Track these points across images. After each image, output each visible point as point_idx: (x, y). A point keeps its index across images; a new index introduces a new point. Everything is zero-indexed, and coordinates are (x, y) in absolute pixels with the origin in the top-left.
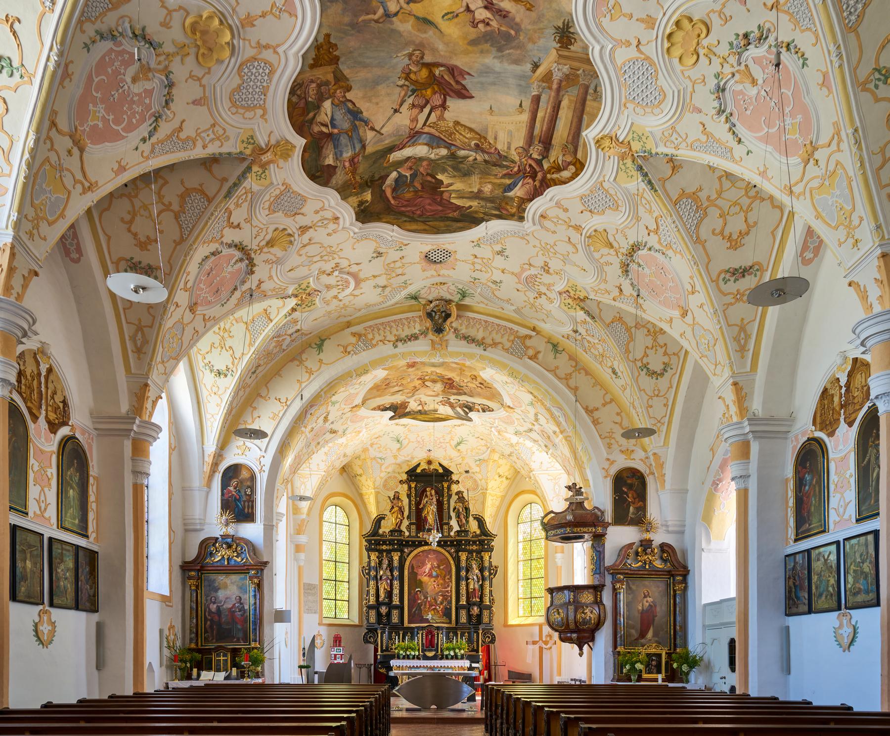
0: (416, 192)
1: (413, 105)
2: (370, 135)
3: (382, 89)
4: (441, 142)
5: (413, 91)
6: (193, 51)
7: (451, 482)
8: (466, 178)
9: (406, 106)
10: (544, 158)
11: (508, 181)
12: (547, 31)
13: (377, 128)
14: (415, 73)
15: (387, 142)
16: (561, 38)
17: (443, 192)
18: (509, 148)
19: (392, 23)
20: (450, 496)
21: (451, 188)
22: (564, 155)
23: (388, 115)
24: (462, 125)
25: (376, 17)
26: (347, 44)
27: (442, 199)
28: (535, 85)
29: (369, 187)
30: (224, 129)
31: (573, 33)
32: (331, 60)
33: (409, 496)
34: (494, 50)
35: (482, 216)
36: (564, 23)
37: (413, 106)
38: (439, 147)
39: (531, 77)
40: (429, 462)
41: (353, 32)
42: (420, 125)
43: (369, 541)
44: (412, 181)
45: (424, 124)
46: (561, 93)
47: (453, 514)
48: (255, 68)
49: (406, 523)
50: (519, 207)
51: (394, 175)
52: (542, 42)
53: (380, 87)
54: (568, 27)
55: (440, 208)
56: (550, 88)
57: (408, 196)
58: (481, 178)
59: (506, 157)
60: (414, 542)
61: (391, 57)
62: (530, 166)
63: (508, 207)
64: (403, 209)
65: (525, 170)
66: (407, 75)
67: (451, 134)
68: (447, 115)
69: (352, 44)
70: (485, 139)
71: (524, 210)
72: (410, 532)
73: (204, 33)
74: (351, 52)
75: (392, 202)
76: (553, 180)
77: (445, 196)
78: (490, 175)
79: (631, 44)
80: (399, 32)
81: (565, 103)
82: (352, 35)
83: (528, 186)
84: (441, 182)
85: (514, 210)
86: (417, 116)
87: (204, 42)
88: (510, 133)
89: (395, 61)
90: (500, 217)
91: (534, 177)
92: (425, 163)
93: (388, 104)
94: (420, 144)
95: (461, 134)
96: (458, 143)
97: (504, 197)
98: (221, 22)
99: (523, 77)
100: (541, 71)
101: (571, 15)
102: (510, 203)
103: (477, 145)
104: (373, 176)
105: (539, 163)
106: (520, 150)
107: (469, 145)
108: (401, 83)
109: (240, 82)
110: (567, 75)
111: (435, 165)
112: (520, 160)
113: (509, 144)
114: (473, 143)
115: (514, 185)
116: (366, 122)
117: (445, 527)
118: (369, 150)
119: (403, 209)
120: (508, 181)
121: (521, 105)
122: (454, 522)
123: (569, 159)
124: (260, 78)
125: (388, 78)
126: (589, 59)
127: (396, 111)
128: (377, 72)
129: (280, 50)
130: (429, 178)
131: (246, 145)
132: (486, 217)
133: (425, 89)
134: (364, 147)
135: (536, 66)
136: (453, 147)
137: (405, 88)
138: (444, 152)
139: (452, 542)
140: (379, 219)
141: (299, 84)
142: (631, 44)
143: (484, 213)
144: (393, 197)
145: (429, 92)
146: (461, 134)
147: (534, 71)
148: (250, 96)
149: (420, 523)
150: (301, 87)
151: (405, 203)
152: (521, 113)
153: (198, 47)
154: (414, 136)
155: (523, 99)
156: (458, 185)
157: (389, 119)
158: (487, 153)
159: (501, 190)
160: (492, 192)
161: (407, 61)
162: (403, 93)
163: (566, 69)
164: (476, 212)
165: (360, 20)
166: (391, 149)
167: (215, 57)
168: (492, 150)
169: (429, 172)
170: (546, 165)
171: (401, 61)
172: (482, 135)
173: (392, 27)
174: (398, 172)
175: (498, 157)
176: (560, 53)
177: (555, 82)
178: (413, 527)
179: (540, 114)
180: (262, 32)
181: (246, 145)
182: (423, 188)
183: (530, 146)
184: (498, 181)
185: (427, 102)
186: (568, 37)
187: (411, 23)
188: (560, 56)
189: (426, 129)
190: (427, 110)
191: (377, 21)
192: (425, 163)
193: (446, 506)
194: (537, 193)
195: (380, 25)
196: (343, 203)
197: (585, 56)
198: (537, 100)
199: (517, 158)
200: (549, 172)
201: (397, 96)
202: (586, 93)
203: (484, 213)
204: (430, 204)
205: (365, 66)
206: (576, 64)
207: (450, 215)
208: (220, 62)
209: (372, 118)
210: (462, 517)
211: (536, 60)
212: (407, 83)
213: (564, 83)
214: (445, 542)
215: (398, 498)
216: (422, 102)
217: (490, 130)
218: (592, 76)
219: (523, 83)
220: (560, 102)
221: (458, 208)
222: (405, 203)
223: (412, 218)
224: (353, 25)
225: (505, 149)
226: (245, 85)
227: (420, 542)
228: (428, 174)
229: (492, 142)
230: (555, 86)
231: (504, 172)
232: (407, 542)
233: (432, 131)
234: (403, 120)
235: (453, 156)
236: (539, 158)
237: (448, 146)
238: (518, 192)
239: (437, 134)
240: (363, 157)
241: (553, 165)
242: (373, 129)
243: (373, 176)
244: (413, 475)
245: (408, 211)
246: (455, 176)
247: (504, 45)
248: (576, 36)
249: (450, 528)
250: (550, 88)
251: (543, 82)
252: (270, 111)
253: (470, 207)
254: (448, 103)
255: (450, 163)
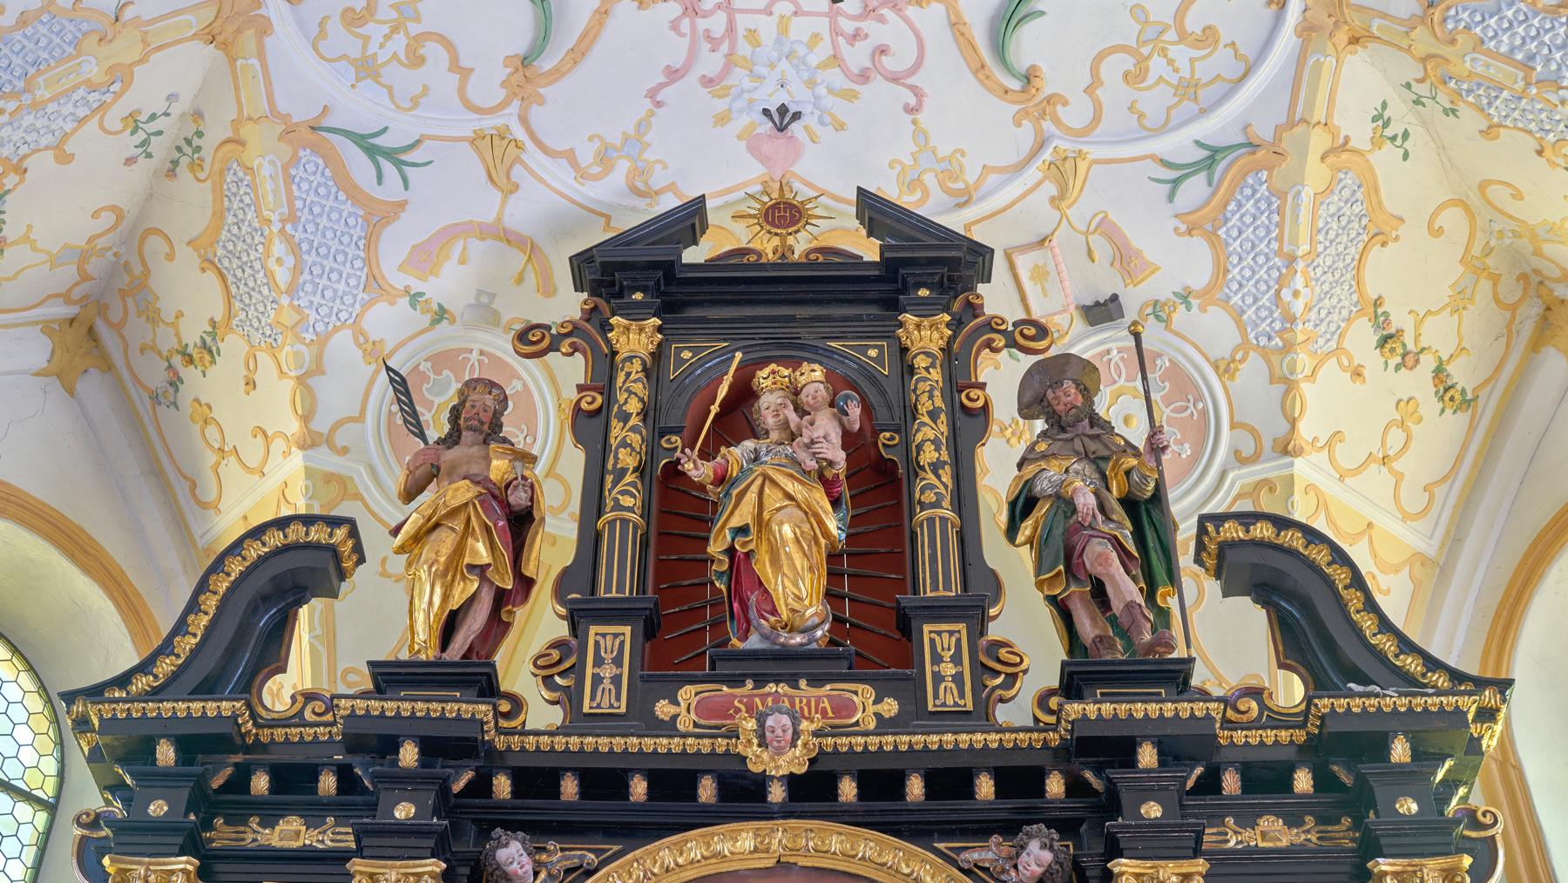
7: (973, 330)
20: (970, 421)
33: (590, 425)
40: (784, 214)
43: (126, 753)
47: (1013, 563)
49: (540, 622)
60: (604, 781)
72: (570, 699)
117: (941, 640)
122: (1027, 625)
139: (1019, 779)
149: (677, 599)
178: (613, 641)
193: (933, 487)
210: (1103, 559)
214: (950, 780)
215: (491, 431)
227: (673, 783)
232: (537, 779)
244: (640, 272)
249: (993, 666)
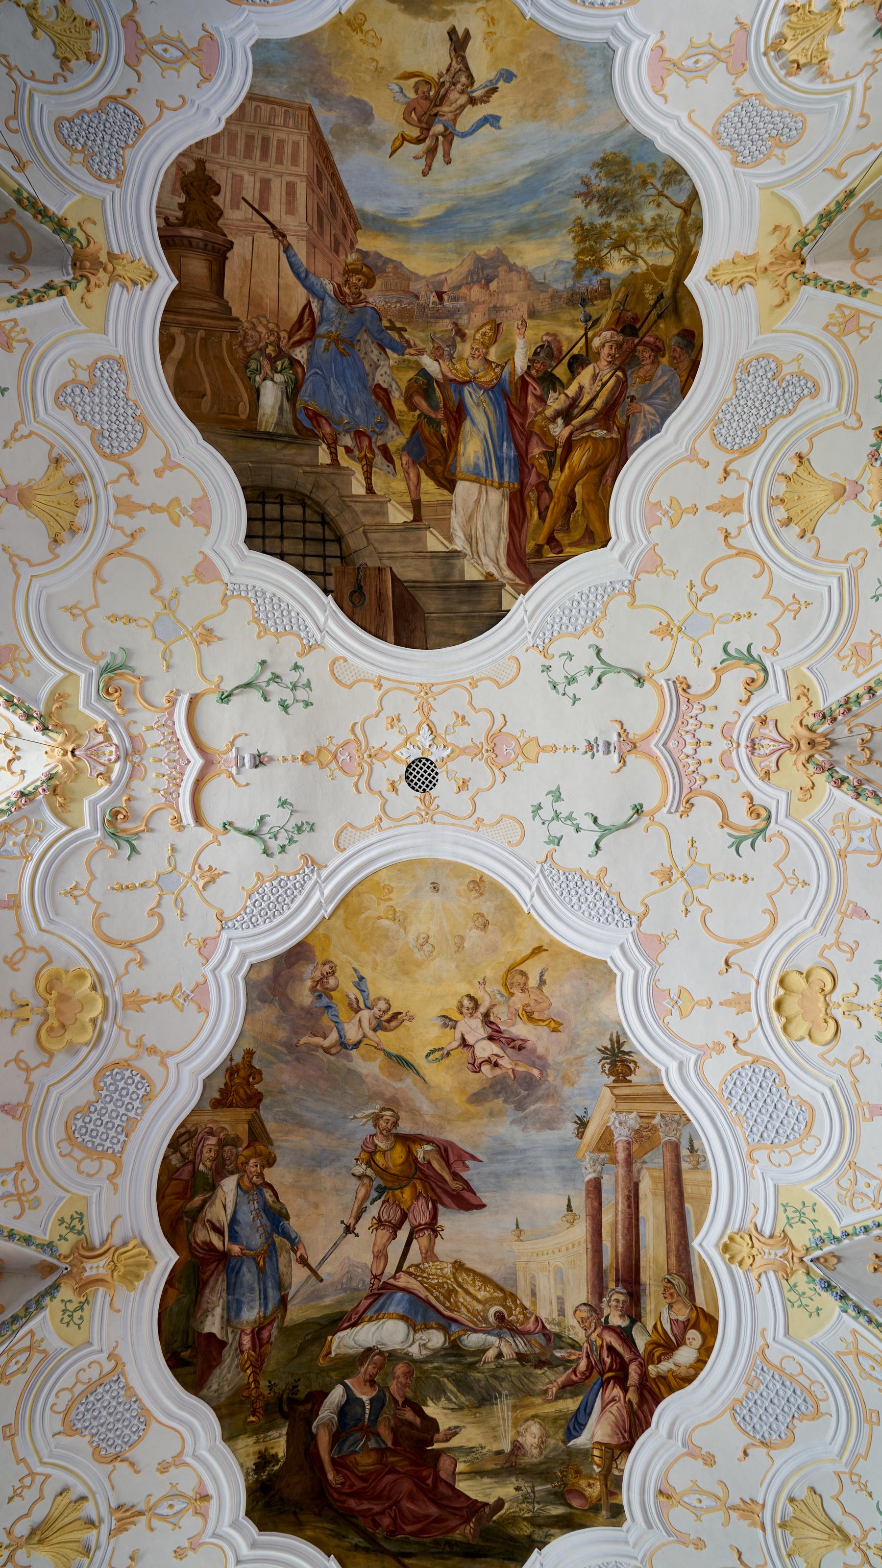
0: (382, 1451)
1: (379, 1220)
2: (298, 1275)
3: (327, 1177)
4: (432, 1313)
5: (381, 1190)
6: (36, 1019)
8: (484, 1411)
9: (366, 1221)
10: (633, 1322)
11: (571, 1405)
12: (588, 1059)
13: (314, 1266)
14: (384, 1153)
15: (329, 1302)
16: (613, 1064)
17: (439, 1453)
18: (562, 1312)
19: (349, 1059)
21: (455, 1442)
22: (670, 1306)
23: (336, 1241)
24: (469, 1271)
25: (326, 1043)
26: (278, 1076)
27: (437, 1479)
28: (587, 1162)
29: (285, 1416)
30: (36, 1181)
31: (628, 1053)
32: (249, 1098)
34: (510, 1107)
35: (526, 1529)
36: (611, 1040)
37: (380, 1223)
38: (427, 1327)
39: (577, 1148)
41: (288, 1058)
42: (391, 1269)
44: (374, 1420)
45: (399, 1269)
46: (636, 1166)
48: (123, 1083)
50: (606, 1474)
51: (337, 1394)
52: (584, 1080)
53: (323, 1172)
54: (620, 1045)
55: (433, 1510)
56: (614, 1161)
57: (366, 1462)
58: (515, 1408)
59: (559, 1336)
61: (345, 1117)
62: (610, 1348)
63: (583, 1483)
64: (352, 1503)
65: (602, 1362)
66: (370, 1155)
67: (451, 1292)
68: (441, 1247)
69: (285, 1077)
70: (514, 1297)
71: (618, 1482)
73: (63, 998)
74: (282, 1092)
75: (331, 1476)
76: (662, 1378)
77: (445, 1463)
78: (530, 1393)
79: (724, 1047)
80: (360, 1076)
81: (645, 1186)
82: (287, 1063)
83: (614, 1408)
84: (432, 1424)
85: (595, 1491)
86: (385, 1247)
87: (59, 1012)
88: (559, 1276)
89: (351, 1125)
90: (568, 1524)
91: (622, 1381)
92: (400, 1369)
93: (336, 1208)
94: (391, 1317)
95: (467, 1292)
96: (463, 1316)
97: (572, 1453)
98: (94, 988)
99: (565, 1150)
100: (592, 1131)
101: (620, 1024)
102: (585, 1471)
103: (500, 1317)
104: (294, 1389)
105: (625, 1335)
106: (584, 1313)
107: (485, 1319)
108: (360, 1169)
109: (93, 1098)
110: (637, 1131)
111: (421, 1375)
112: (588, 1337)
113: (561, 1301)
114: (492, 1311)
115: (586, 1410)
116: (294, 1243)
118: (295, 1314)
119: (352, 1503)
120: (571, 1405)
121: (569, 1208)
123: (682, 1313)
124: (127, 1100)
125: (338, 1157)
126: (666, 1094)
127: (349, 1230)
128: (321, 1140)
129: (171, 1062)
130: (409, 1415)
131: (64, 1231)
132: (538, 1535)
133: (401, 1188)
134: (283, 1302)
135: (582, 1124)
136: (454, 1327)
137: (366, 1181)
138: (436, 1339)
140: (296, 1528)
141: (188, 1132)
142: (724, 1047)
143: (531, 1521)
144: (333, 1461)
145: (407, 1194)
146: (467, 1292)
147: (580, 1135)
148: (102, 1129)
150: (191, 1138)
151: (359, 1485)
152: (572, 1223)
153: (47, 1016)
154: (378, 1295)
155: (572, 1193)
156: (471, 1435)
157: (336, 1245)
158: (522, 1334)
159: (561, 1435)
160: (542, 1443)
161: (370, 1129)
162: (362, 1193)
163: (632, 1120)
164: (513, 1520)
165: (302, 1041)
166: (337, 1322)
167: (68, 1036)
168: (530, 1325)
169: (410, 1395)
170: (641, 1342)
171: (361, 1128)
172: (508, 1289)
173: (349, 1065)
174: (346, 1387)
175: (542, 1340)
176: (616, 1091)
177: (621, 1147)
179: (607, 1218)
180: (149, 1024)
181: (64, 1231)
182: (395, 1442)
183: (601, 1296)
184: (549, 1409)
185: (404, 1217)
186: (623, 1061)
187: (378, 1061)
188: (618, 1097)
189: (403, 1281)
190: (403, 1234)
191: (327, 1051)
192: (400, 1369)
194: (635, 1424)
195: (332, 1058)
196: (224, 1448)
197: (658, 1090)
198: (595, 1188)
199: (580, 1335)
200: (651, 1358)
201: (351, 1196)
202: (677, 1157)
203: (531, 1521)
204: (411, 1498)
205: (303, 1124)
206: (647, 1107)
207: (457, 1536)
208: (72, 1049)
209: (306, 1237)
211: (580, 1113)
212: (369, 1172)
213: (635, 1147)
216: (394, 1215)
217: (520, 1275)
218: (679, 1124)
219: (565, 1162)
220: (637, 1185)
221: (475, 1508)
222: (359, 1485)
223: (370, 1539)
224: (291, 1047)
225: (555, 1315)
226: (99, 1105)
228: (407, 1402)
229: (527, 1304)
230: (621, 1156)
231: (561, 1379)
233: (414, 1284)
234: (360, 1250)
235: (454, 1350)
236: (624, 1323)
237: (446, 1323)
238: (598, 1430)
239: (423, 1293)
240: (281, 1329)
241: (655, 1337)
242: (303, 1261)
243: (294, 1389)
245: (363, 1514)
246: (461, 1408)
247: (525, 1098)
248: (635, 1057)
250: (614, 1161)
251: (600, 1151)
252: (128, 1169)
253: (500, 1504)
254: (441, 1221)
255: (450, 1369)
